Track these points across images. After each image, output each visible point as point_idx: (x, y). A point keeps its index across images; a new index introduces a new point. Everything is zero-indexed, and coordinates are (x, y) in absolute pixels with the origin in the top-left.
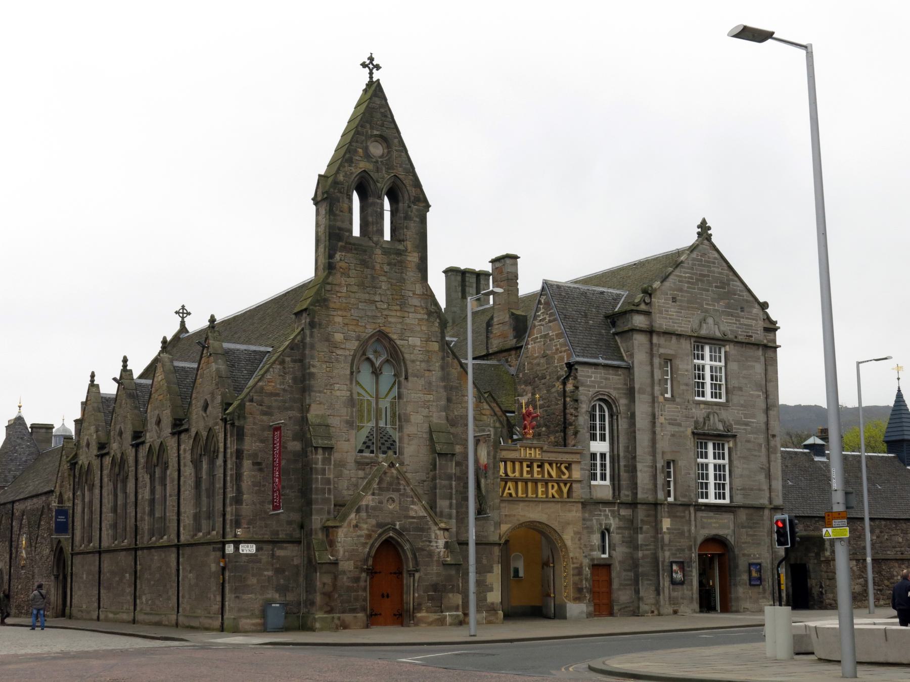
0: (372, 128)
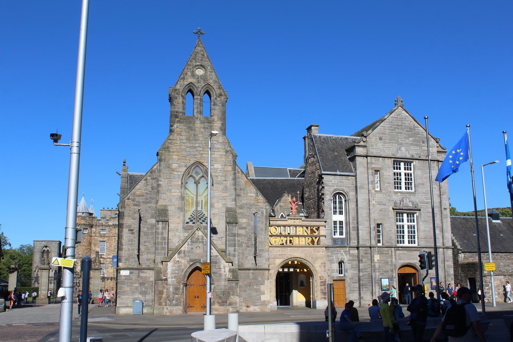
0: (196, 62)
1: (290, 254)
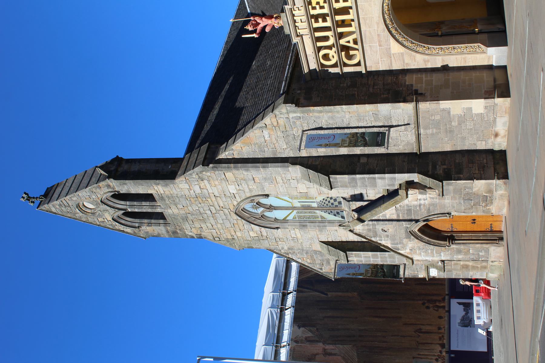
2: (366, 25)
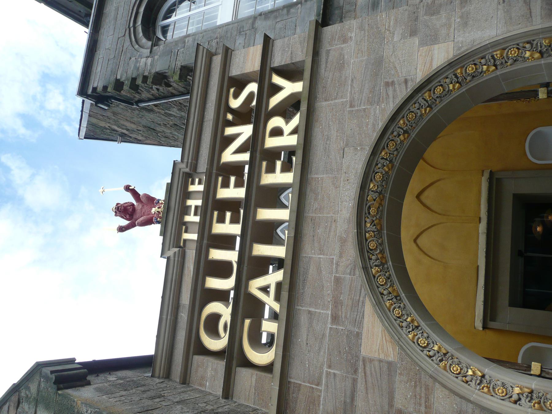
1: (337, 251)
2: (313, 241)
